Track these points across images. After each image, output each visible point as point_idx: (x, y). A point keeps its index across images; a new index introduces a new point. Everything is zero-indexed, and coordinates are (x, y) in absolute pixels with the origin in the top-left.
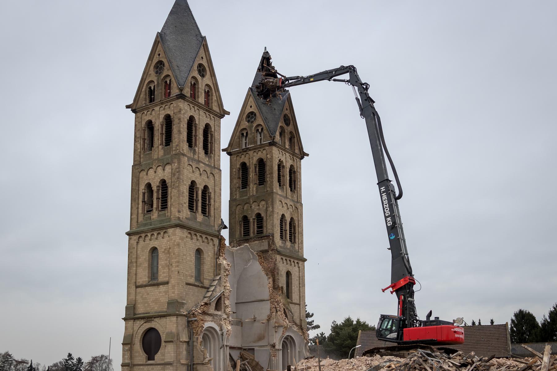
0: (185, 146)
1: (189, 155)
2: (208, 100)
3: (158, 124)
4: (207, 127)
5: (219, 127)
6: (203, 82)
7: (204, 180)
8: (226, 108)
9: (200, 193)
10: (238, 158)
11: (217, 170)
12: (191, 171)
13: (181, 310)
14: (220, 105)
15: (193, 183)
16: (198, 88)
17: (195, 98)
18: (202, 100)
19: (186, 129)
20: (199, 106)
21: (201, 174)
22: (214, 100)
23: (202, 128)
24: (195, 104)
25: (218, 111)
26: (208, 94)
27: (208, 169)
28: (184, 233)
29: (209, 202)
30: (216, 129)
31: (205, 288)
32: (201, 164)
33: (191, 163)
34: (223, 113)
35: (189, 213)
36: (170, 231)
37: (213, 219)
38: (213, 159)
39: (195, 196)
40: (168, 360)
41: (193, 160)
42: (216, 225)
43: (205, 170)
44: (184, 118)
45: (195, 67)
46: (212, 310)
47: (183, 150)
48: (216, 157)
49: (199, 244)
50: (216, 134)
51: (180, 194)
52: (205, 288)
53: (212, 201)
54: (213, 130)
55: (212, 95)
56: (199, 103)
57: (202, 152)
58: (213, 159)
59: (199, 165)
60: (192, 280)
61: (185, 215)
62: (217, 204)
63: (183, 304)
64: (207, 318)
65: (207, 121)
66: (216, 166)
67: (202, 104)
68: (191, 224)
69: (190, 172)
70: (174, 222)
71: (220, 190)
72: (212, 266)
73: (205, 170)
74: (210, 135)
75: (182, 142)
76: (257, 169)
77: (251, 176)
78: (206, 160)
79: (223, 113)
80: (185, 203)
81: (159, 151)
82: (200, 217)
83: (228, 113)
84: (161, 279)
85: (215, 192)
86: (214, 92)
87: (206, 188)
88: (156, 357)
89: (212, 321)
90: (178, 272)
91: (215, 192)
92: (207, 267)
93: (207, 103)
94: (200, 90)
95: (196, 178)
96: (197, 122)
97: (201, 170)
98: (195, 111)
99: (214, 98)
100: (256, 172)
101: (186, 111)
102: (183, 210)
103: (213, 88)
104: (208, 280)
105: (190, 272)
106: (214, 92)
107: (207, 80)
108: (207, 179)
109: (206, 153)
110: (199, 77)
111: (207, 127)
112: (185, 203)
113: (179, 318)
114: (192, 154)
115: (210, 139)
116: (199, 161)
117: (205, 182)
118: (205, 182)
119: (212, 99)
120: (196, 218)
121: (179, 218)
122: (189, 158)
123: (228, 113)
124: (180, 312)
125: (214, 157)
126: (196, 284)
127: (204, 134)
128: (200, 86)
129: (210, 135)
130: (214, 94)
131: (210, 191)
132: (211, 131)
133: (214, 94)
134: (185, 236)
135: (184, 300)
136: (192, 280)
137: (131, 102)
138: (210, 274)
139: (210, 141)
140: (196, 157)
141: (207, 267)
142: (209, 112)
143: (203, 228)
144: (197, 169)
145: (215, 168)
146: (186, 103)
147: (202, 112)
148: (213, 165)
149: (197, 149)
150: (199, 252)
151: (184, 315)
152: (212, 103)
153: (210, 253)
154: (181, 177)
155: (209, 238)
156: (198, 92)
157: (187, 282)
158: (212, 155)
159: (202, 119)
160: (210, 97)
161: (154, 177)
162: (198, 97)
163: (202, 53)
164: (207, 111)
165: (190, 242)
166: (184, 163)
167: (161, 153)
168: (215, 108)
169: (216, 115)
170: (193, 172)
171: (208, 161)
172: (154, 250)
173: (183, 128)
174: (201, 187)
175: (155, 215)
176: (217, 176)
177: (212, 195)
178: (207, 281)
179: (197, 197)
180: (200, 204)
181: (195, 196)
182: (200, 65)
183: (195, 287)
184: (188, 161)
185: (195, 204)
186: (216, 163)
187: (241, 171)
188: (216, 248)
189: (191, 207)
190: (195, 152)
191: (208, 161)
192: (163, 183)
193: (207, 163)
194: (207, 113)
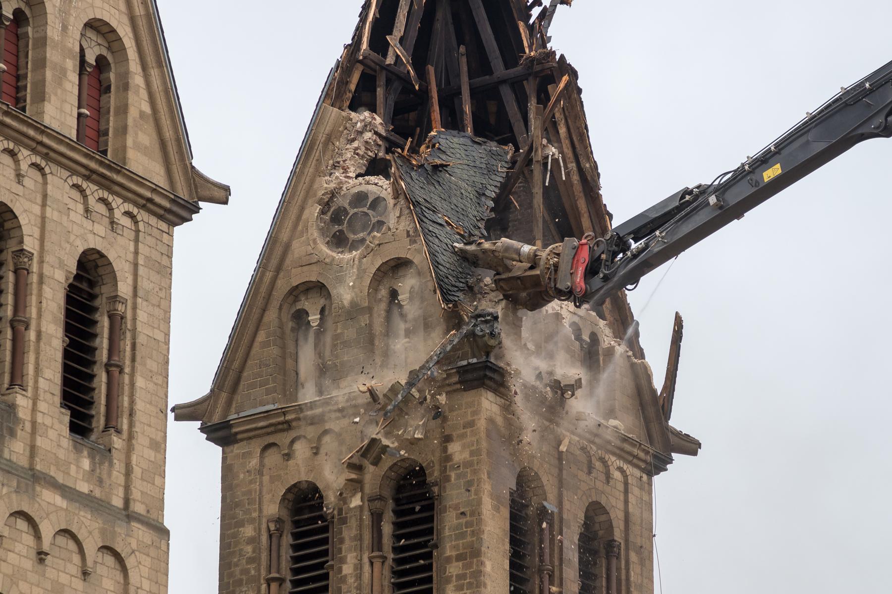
2: (100, 112)
4: (91, 271)
5: (165, 271)
8: (206, 161)
10: (273, 458)
11: (141, 533)
14: (174, 143)
16: (42, 42)
17: (19, 101)
18: (60, 110)
20: (47, 149)
21: (41, 556)
22: (133, 113)
24: (21, 139)
25: (158, 177)
27: (89, 528)
30: (144, 284)
32: (49, 497)
34: (187, 195)
38: (119, 466)
43: (66, 532)
48: (142, 454)
50: (142, 316)
54: (124, 289)
55: (126, 87)
56: (44, 130)
57: (54, 420)
58: (119, 466)
59: (33, 497)
65: (91, 235)
66: (138, 508)
67: (60, 138)
73: (66, 532)
74: (105, 322)
76: (387, 529)
77: (347, 569)
79: (187, 195)
83: (221, 195)
86: (134, 65)
93: (95, 129)
94: (52, 55)
96: (30, 244)
97: (47, 530)
98: (19, 176)
99: (138, 103)
100: (377, 544)
103: (129, 42)
106: (134, 65)
108: (78, 584)
109: (80, 427)
111: (91, 271)
115: (103, 343)
116: (33, 477)
119: (123, 110)
123: (221, 195)
125: (129, 449)
127: (69, 314)
128: (53, 31)
129: (105, 322)
132: (114, 299)
133: (137, 80)
139: (103, 355)
142: (105, 183)
144: (22, 524)
147: (60, 184)
148: (117, 502)
152: (123, 130)
156: (41, 63)
158: (118, 442)
159: (60, 226)
160: (113, 99)
162: (41, 97)
164: (90, 175)
168: (143, 161)
169: (147, 205)
186: (138, 488)
187: (287, 540)
191: (93, 475)
193: (84, 487)
194: (90, 187)
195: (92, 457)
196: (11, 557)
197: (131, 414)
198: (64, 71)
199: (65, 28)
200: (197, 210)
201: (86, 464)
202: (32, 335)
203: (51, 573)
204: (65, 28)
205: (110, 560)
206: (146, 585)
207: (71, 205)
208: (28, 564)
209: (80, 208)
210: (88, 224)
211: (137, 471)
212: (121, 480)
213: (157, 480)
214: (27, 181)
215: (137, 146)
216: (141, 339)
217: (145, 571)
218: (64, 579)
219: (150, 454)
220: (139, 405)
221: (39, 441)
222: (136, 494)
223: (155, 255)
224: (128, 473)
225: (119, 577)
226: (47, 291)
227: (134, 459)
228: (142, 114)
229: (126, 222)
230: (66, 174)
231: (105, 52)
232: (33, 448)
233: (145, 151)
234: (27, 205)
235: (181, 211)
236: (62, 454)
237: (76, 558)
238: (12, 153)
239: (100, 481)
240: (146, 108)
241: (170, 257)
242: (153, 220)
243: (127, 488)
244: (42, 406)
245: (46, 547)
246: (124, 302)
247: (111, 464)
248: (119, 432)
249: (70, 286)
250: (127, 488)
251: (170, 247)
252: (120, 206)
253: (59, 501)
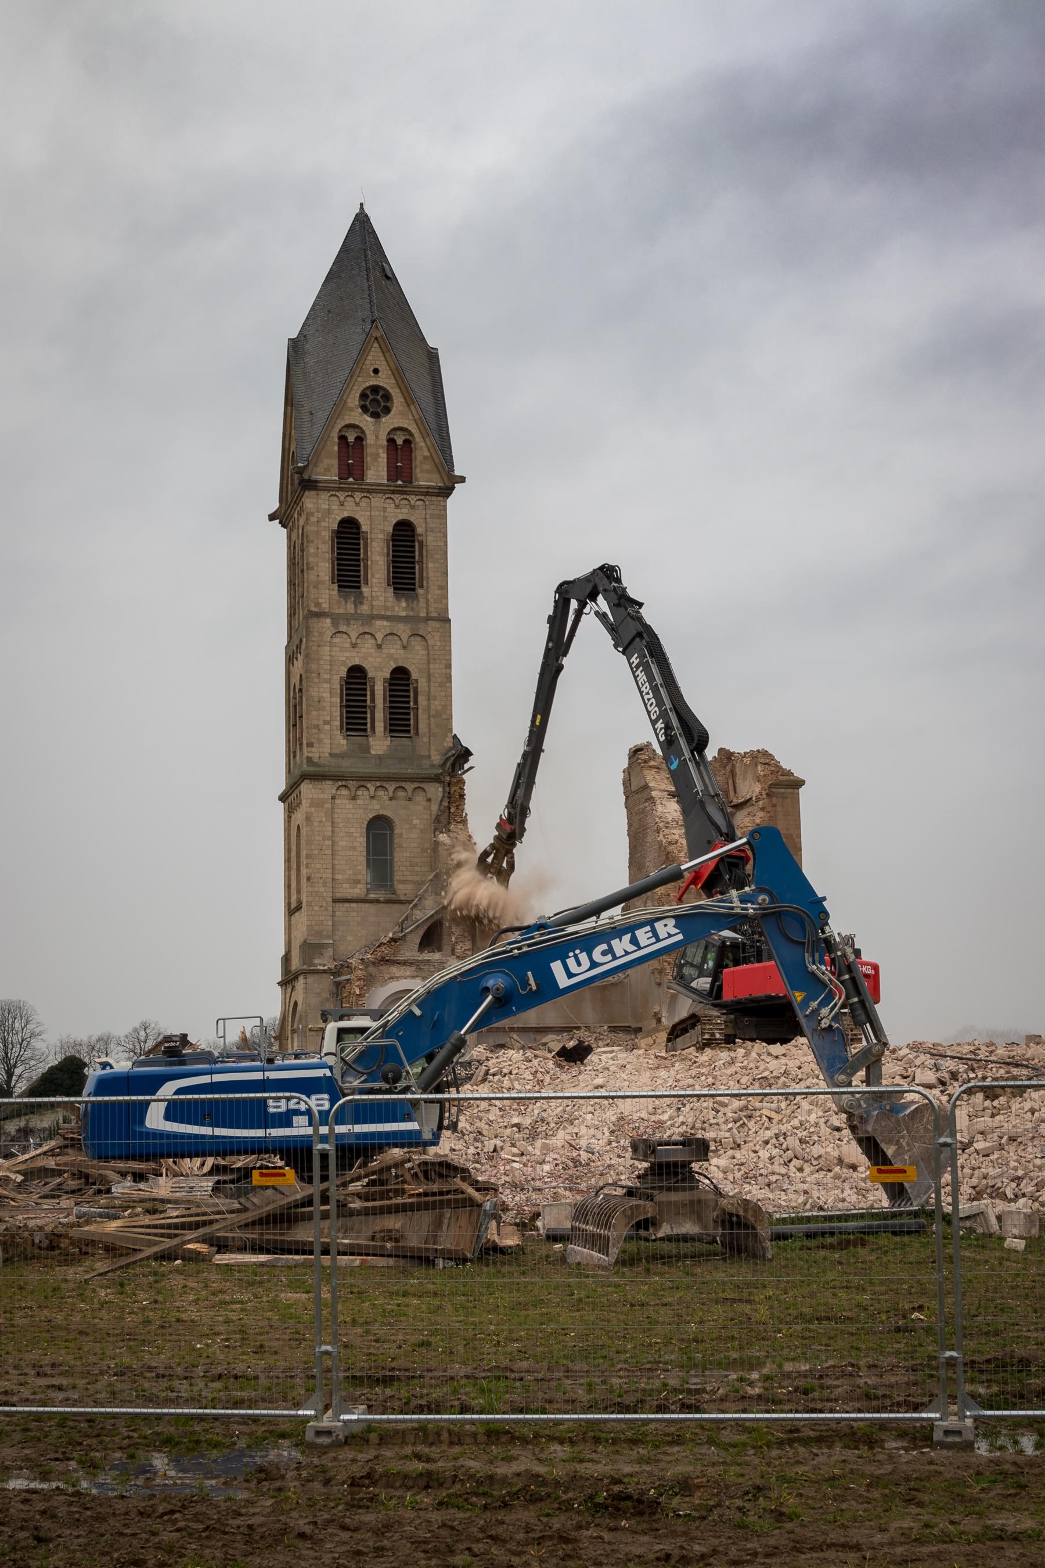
1: (342, 611)
5: (442, 516)
6: (376, 433)
7: (390, 656)
9: (379, 689)
11: (437, 625)
12: (347, 645)
13: (316, 961)
19: (328, 556)
21: (379, 647)
22: (419, 458)
23: (381, 536)
26: (400, 451)
27: (404, 630)
28: (328, 788)
29: (416, 702)
31: (401, 902)
32: (379, 623)
33: (343, 628)
35: (344, 742)
37: (426, 740)
39: (368, 698)
41: (348, 619)
42: (433, 753)
44: (318, 533)
45: (354, 400)
46: (410, 951)
47: (318, 604)
48: (434, 592)
49: (377, 807)
50: (430, 538)
52: (401, 902)
53: (422, 701)
60: (359, 891)
61: (327, 750)
62: (436, 705)
63: (322, 946)
64: (394, 970)
68: (347, 766)
69: (343, 649)
71: (449, 666)
72: (424, 850)
75: (316, 587)
78: (401, 608)
80: (326, 723)
82: (380, 743)
83: (462, 479)
85: (429, 675)
89: (413, 977)
90: (308, 879)
91: (429, 675)
92: (405, 854)
95: (365, 658)
101: (329, 512)
102: (320, 741)
103: (413, 431)
104: (414, 883)
105: (350, 872)
107: (398, 417)
108: (402, 652)
110: (367, 422)
112: (326, 723)
113: (311, 979)
114: (350, 608)
117: (396, 660)
118: (396, 660)
120: (367, 749)
121: (309, 760)
122: (336, 619)
124: (315, 965)
126: (372, 896)
129: (417, 544)
130: (422, 444)
131: (414, 676)
134: (327, 796)
135: (328, 937)
136: (357, 891)
137: (275, 505)
138: (418, 869)
140: (365, 609)
141: (405, 854)
143: (394, 769)
145: (428, 618)
146: (324, 495)
149: (365, 590)
151: (324, 972)
153: (415, 822)
154: (314, 667)
155: (410, 786)
157: (338, 895)
158: (420, 591)
159: (377, 517)
163: (375, 357)
165: (351, 806)
166: (321, 634)
169: (427, 494)
170: (354, 646)
171: (405, 609)
173: (316, 555)
174: (379, 674)
176: (434, 640)
177: (422, 685)
178: (410, 887)
179: (373, 700)
180: (380, 715)
181: (368, 698)
182: (375, 389)
183: (367, 905)
184: (335, 624)
185: (369, 716)
188: (435, 807)
190: (359, 600)
195: (407, 601)
196: (363, 650)
197: (428, 578)
198: (378, 455)
199: (377, 437)
200: (453, 488)
201: (404, 604)
202: (369, 563)
203: (385, 651)
204: (377, 437)
205: (418, 638)
206: (438, 644)
207: (386, 505)
208: (373, 650)
209: (393, 505)
210: (399, 511)
211: (431, 600)
212: (425, 605)
213: (444, 601)
214: (362, 504)
215: (422, 471)
216: (430, 548)
217: (437, 638)
218: (392, 651)
219: (440, 592)
220: (431, 574)
221: (374, 603)
222: (431, 609)
223: (436, 512)
224: (428, 601)
225: (424, 643)
226: (374, 544)
227: (429, 596)
228: (425, 458)
229: (421, 503)
230: (380, 495)
231: (408, 437)
232: (372, 606)
233: (428, 472)
234: (362, 513)
235: (446, 491)
236: (389, 604)
237: (399, 642)
238: (352, 496)
239: (413, 609)
240: (427, 454)
241: (446, 510)
242: (434, 498)
243: (427, 608)
244: (375, 589)
245: (379, 642)
246: (422, 535)
247: (418, 601)
248: (422, 587)
249: (393, 535)
250: (427, 608)
251: (445, 506)
252: (413, 499)
253: (385, 623)
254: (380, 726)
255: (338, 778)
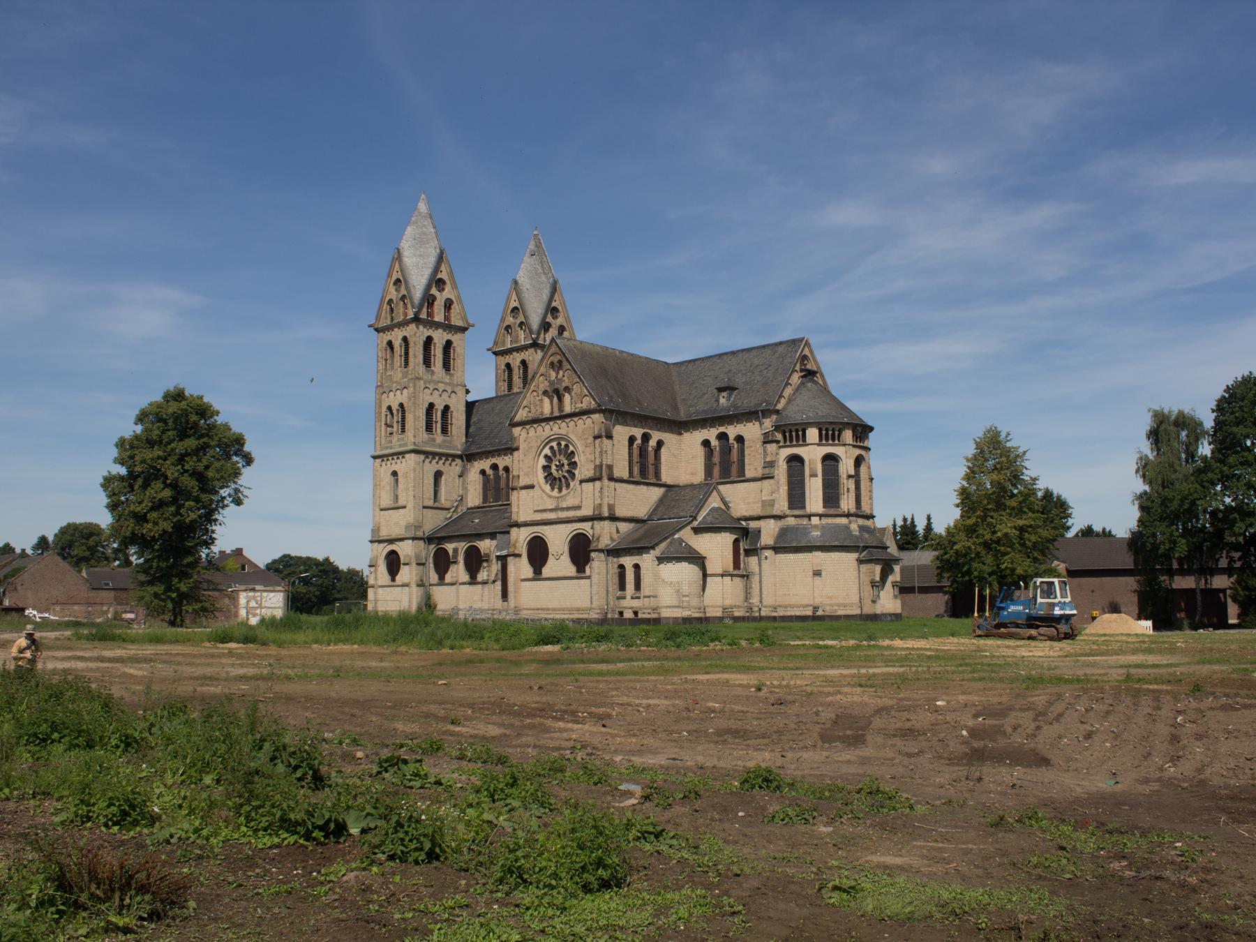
0: (421, 369)
3: (397, 343)
9: (439, 413)
15: (431, 406)
36: (407, 456)
40: (406, 580)
51: (416, 418)
60: (431, 503)
70: (412, 447)
81: (398, 374)
82: (439, 437)
84: (401, 502)
87: (447, 408)
88: (397, 578)
120: (434, 440)
150: (438, 475)
161: (394, 400)
167: (400, 375)
172: (395, 474)
174: (439, 408)
175: (395, 438)
180: (439, 425)
189: (429, 428)
192: (401, 405)
254: (439, 430)
255: (426, 454)
